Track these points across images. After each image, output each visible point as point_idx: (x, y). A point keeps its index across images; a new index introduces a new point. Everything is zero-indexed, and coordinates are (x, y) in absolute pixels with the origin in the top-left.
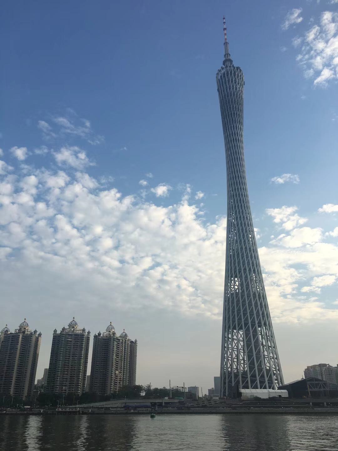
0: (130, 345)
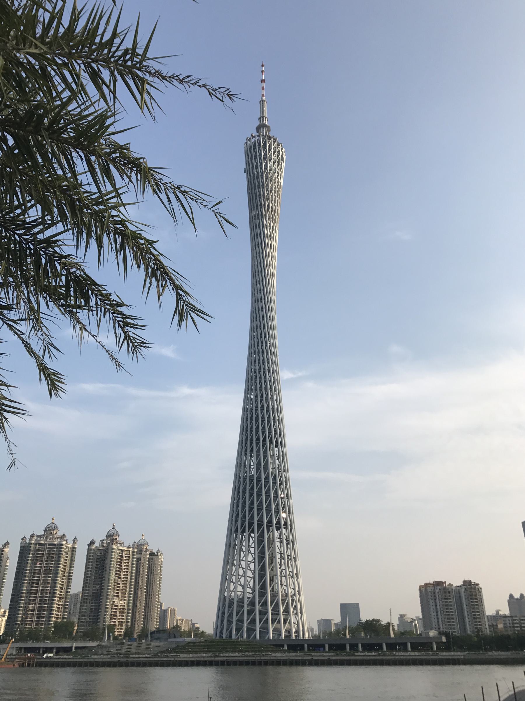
0: (148, 558)
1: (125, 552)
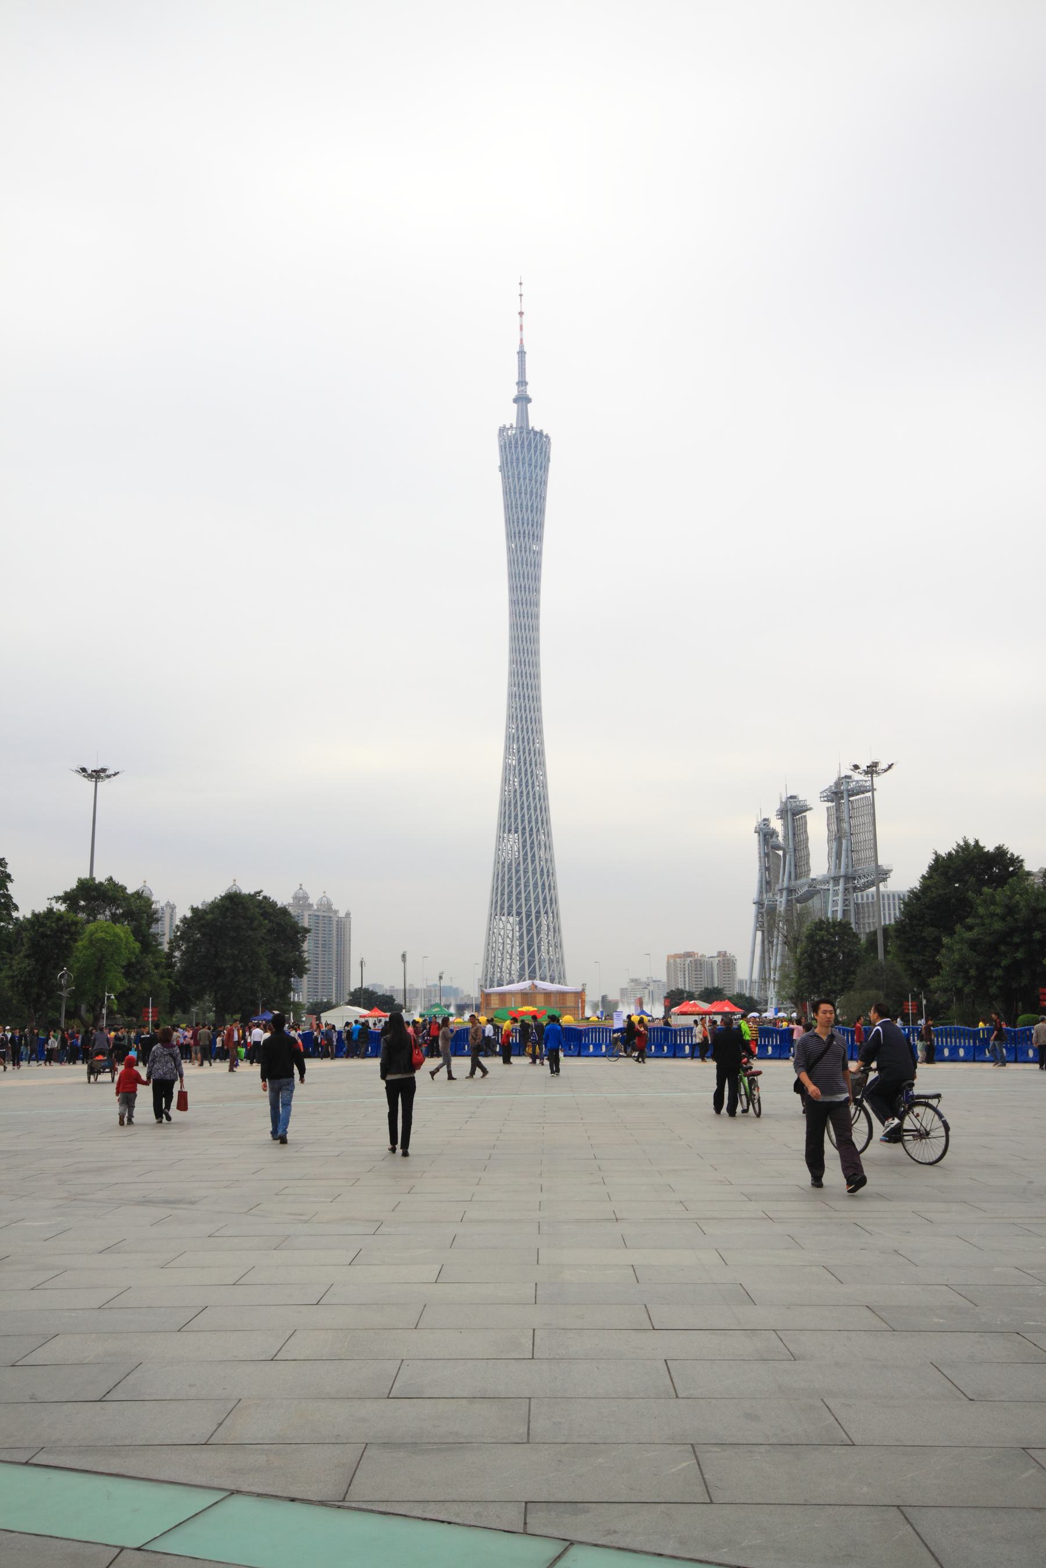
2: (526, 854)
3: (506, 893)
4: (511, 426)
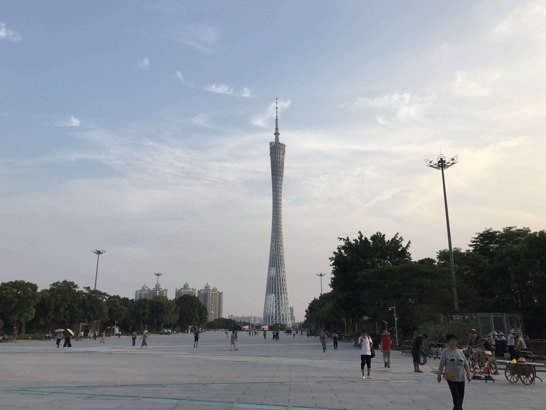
1: (213, 294)
2: (277, 274)
3: (271, 286)
4: (273, 142)
